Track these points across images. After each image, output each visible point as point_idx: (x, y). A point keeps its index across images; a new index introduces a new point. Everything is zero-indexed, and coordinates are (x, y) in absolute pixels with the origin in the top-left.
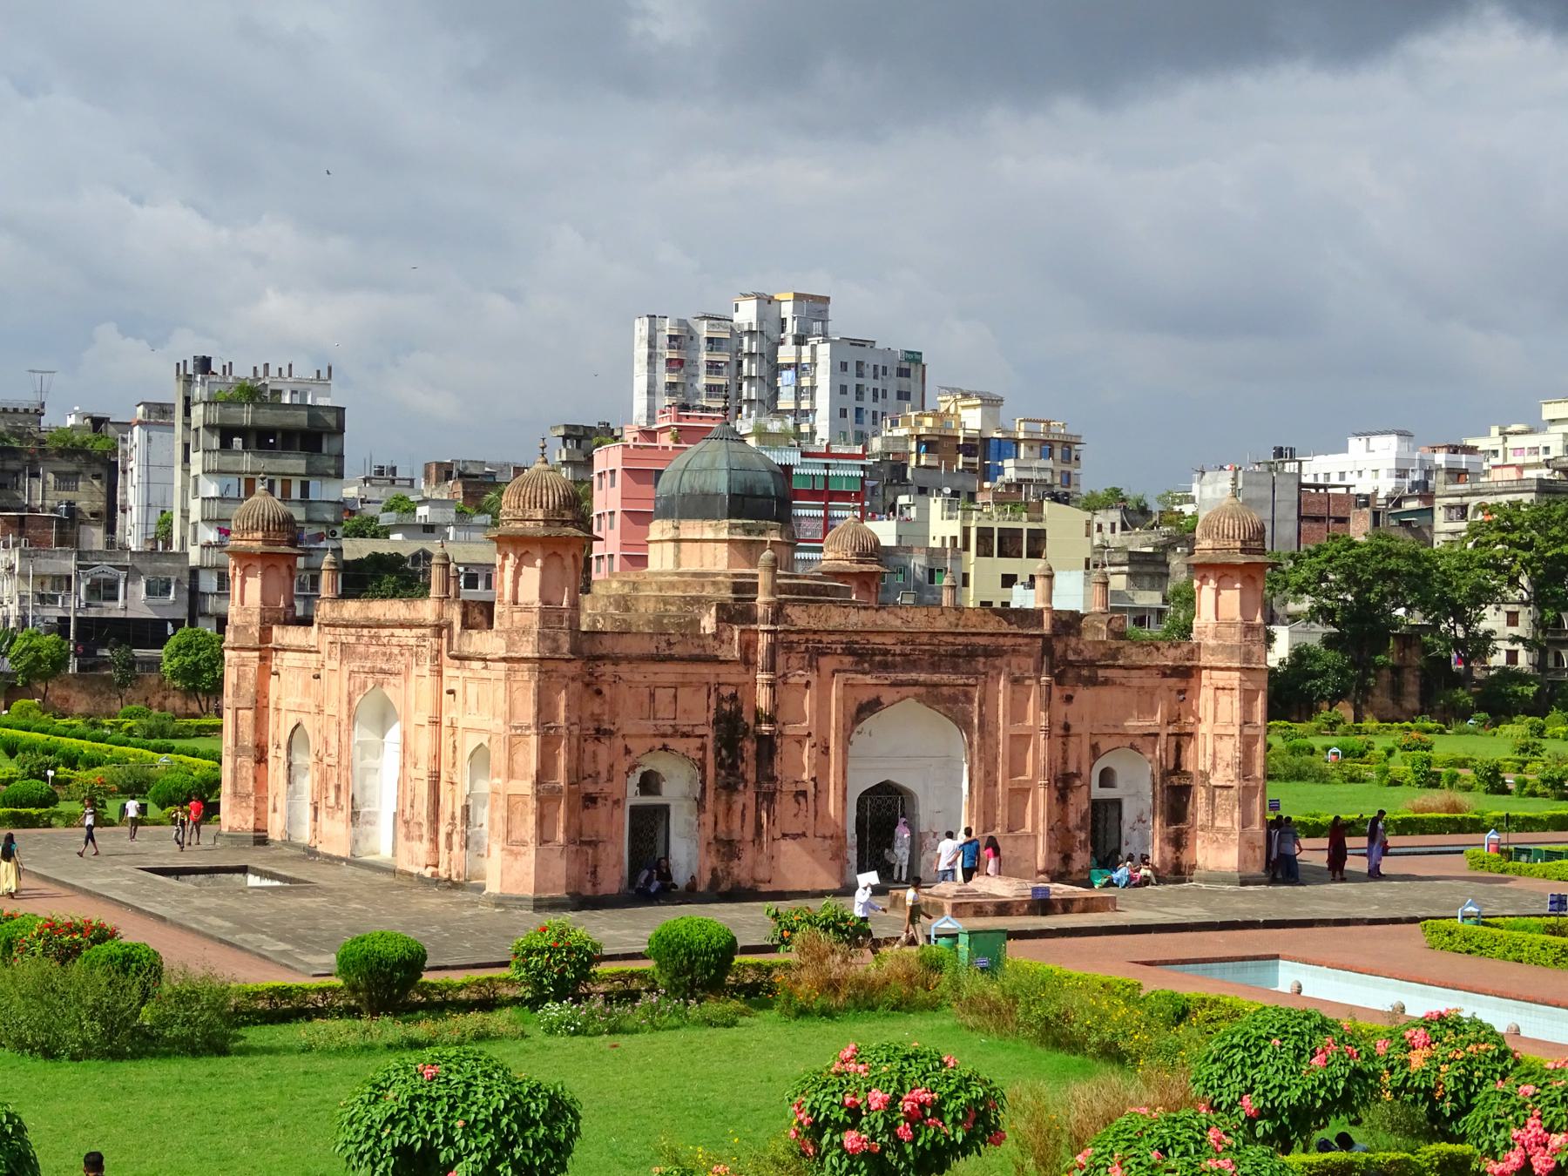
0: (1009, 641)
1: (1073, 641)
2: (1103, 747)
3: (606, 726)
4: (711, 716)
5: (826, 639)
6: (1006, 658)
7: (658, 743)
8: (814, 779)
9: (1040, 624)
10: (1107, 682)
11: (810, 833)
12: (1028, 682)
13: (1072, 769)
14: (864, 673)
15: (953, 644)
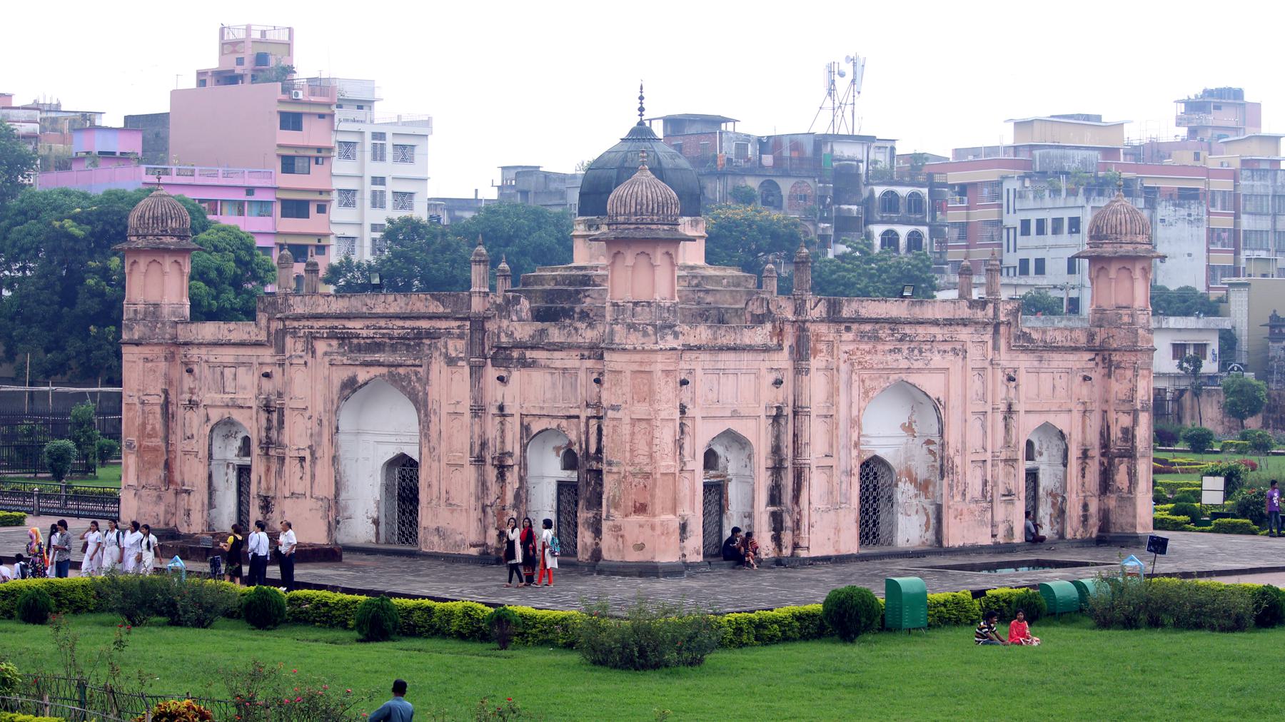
0: (442, 324)
1: (505, 323)
2: (536, 427)
3: (194, 398)
4: (255, 391)
5: (317, 324)
6: (442, 340)
7: (226, 413)
8: (310, 447)
9: (469, 307)
10: (533, 364)
11: (308, 494)
12: (460, 363)
13: (508, 448)
14: (343, 355)
15: (403, 328)
